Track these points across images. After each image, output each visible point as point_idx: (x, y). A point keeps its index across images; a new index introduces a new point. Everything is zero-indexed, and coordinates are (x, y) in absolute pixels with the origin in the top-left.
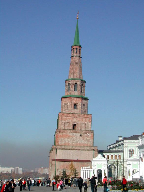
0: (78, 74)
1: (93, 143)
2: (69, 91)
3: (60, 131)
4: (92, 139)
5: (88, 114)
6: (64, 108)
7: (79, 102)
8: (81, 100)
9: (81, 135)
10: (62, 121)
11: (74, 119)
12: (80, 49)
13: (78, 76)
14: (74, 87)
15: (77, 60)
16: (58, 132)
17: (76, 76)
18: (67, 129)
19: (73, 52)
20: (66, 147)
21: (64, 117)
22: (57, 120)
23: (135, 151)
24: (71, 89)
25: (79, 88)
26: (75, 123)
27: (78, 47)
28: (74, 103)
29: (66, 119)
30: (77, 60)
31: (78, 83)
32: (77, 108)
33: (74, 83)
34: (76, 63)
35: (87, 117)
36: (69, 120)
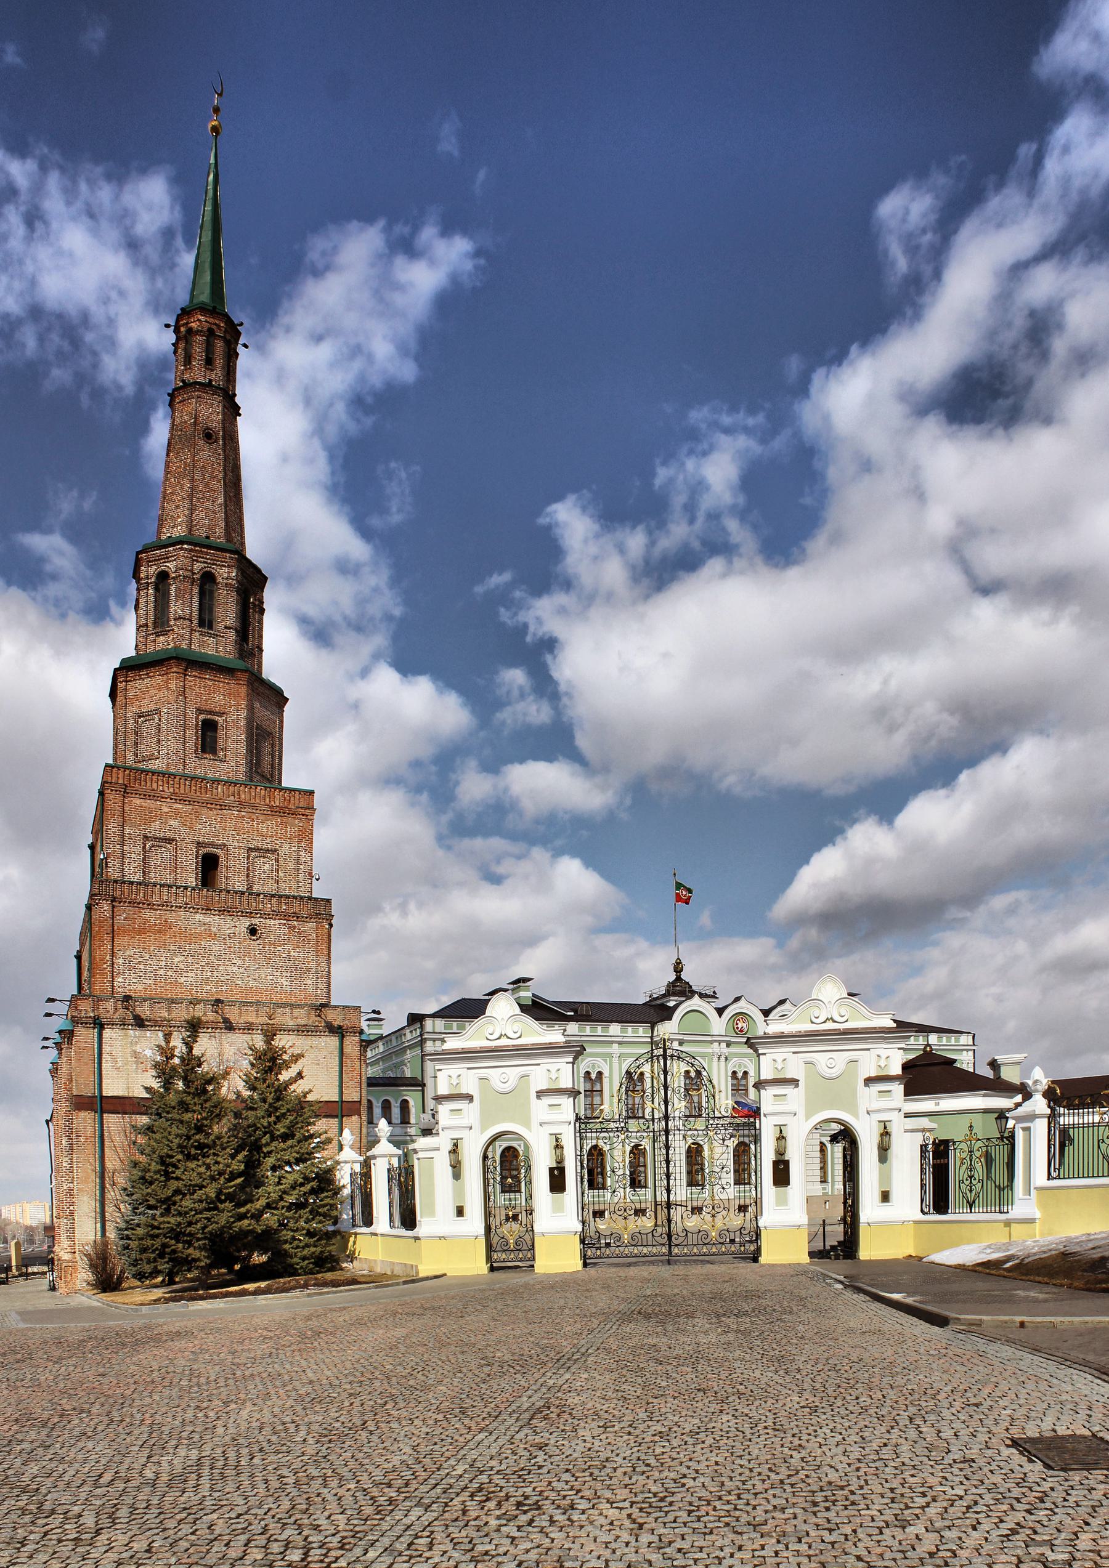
0: (220, 515)
1: (329, 985)
2: (160, 623)
3: (117, 894)
4: (323, 959)
5: (284, 784)
7: (231, 705)
8: (243, 690)
9: (253, 931)
13: (220, 531)
14: (196, 599)
15: (211, 412)
16: (106, 906)
17: (210, 522)
18: (162, 886)
19: (188, 360)
21: (138, 802)
24: (176, 608)
25: (227, 612)
28: (199, 711)
29: (152, 816)
32: (221, 744)
36: (175, 823)
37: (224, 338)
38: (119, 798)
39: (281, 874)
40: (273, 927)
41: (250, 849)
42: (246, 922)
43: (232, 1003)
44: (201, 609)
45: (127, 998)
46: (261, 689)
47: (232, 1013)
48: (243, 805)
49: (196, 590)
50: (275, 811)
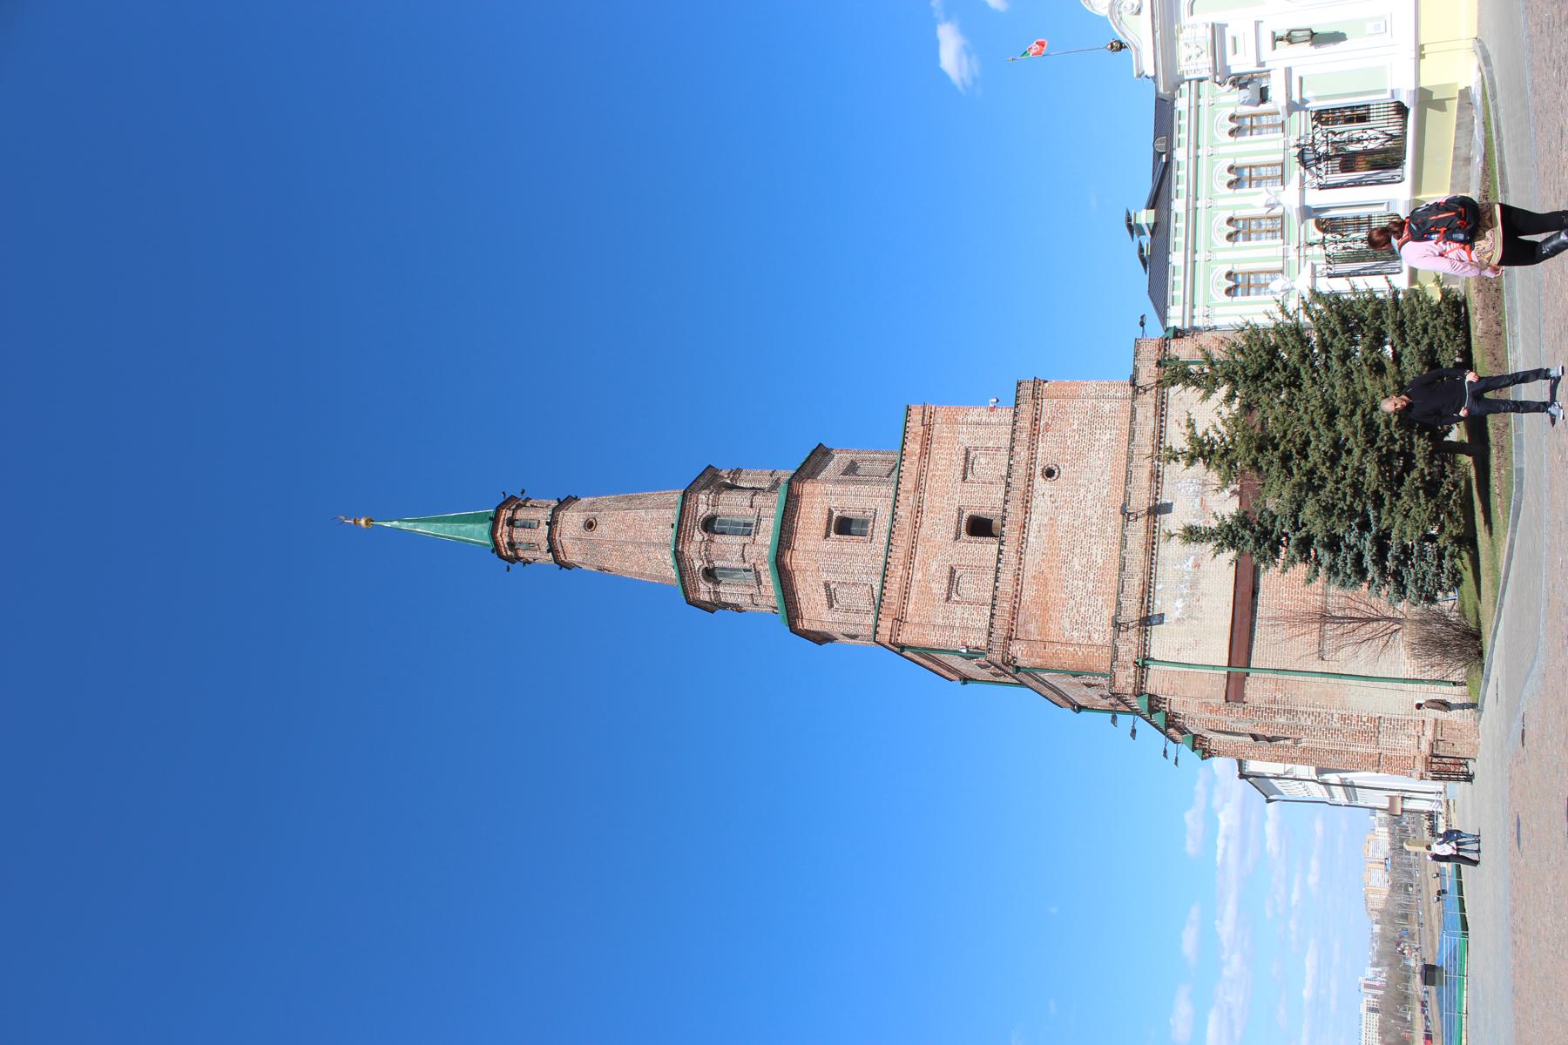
0: (655, 513)
6: (858, 612)
7: (820, 500)
9: (1049, 473)
10: (940, 621)
11: (923, 531)
12: (519, 507)
14: (725, 538)
20: (1134, 586)
21: (911, 606)
22: (970, 685)
23: (1233, 262)
26: (959, 522)
27: (506, 514)
28: (827, 535)
30: (575, 519)
31: (703, 510)
33: (698, 536)
34: (590, 525)
35: (926, 442)
37: (514, 511)
38: (907, 628)
39: (991, 444)
40: (1047, 452)
41: (964, 479)
42: (1039, 481)
43: (1127, 495)
44: (735, 533)
45: (1117, 625)
46: (808, 469)
47: (1141, 501)
48: (918, 487)
49: (717, 538)
50: (925, 451)
